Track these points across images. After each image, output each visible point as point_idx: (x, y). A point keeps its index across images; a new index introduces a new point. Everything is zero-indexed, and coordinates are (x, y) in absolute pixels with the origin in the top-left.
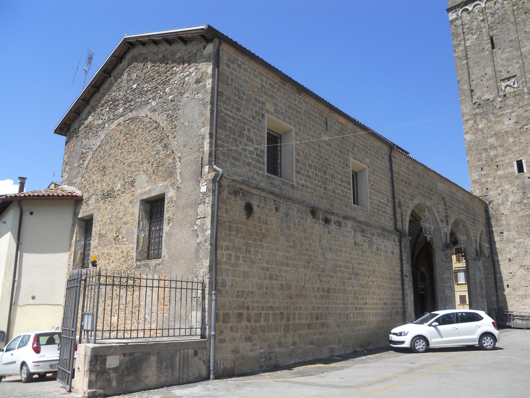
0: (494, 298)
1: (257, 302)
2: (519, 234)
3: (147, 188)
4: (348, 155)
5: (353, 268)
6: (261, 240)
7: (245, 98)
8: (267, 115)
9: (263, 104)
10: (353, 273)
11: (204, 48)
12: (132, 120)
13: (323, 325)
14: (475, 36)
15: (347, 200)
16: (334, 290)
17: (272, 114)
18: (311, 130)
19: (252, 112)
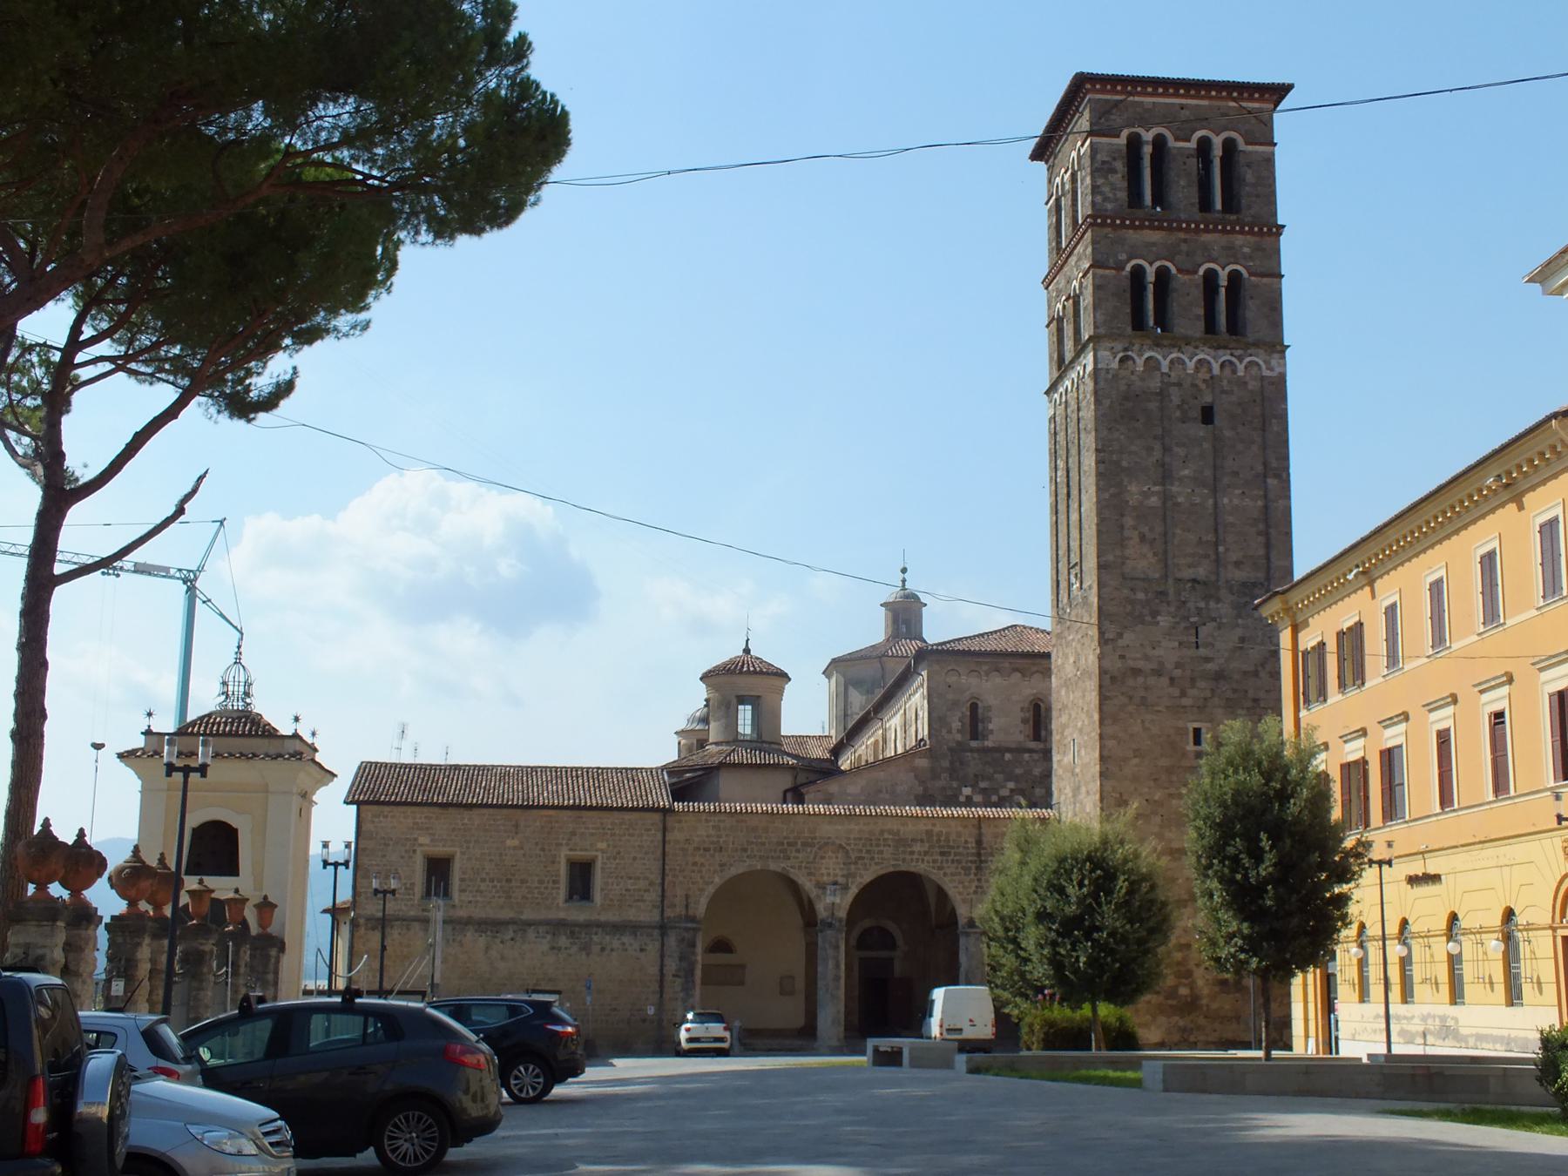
8: (419, 850)
9: (416, 839)
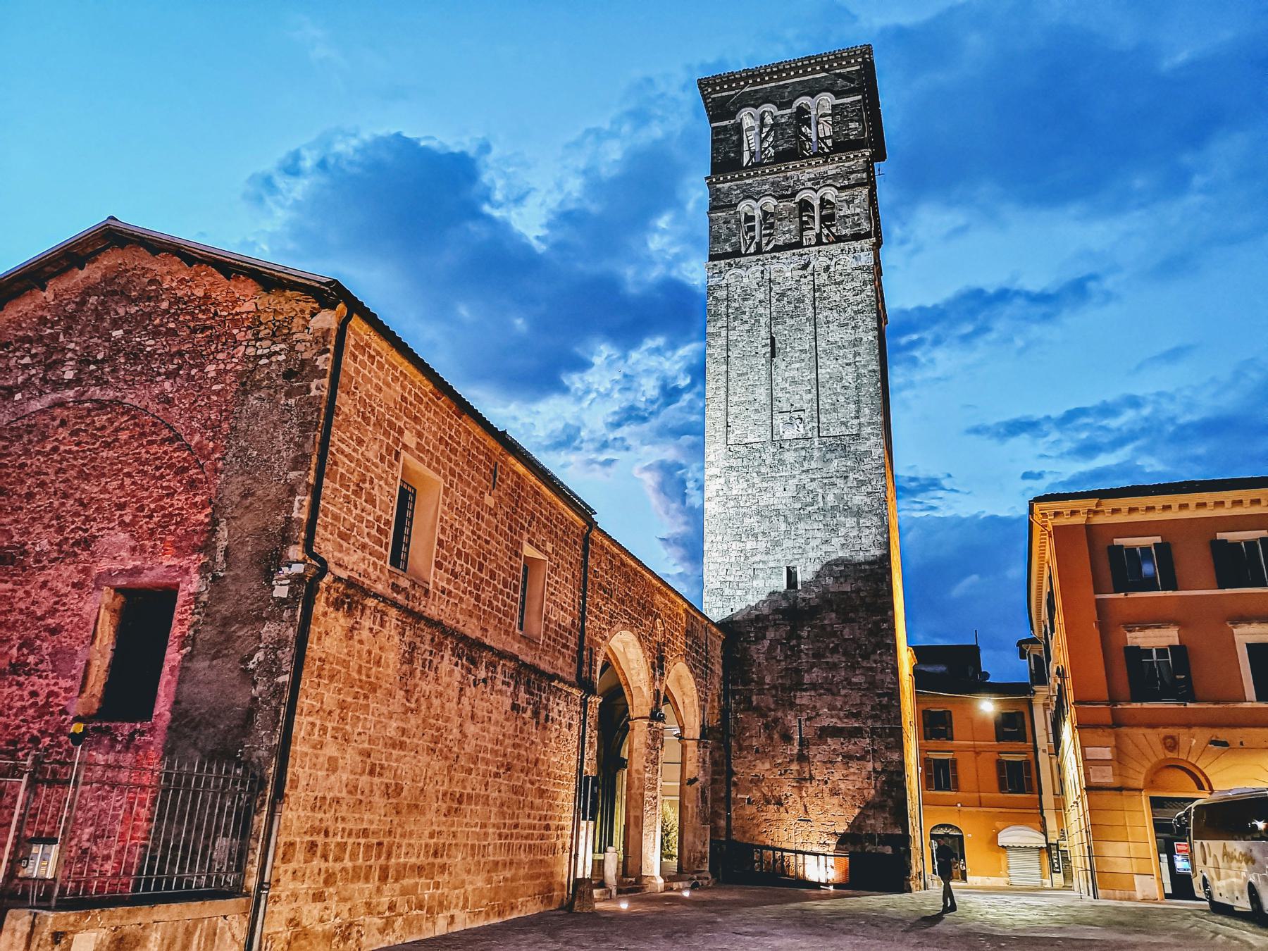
0: (723, 823)
1: (343, 819)
2: (776, 703)
3: (130, 566)
4: (521, 535)
5: (505, 755)
6: (366, 697)
7: (373, 419)
9: (401, 432)
10: (503, 765)
11: (313, 315)
12: (101, 405)
13: (443, 868)
14: (747, 327)
15: (508, 620)
16: (470, 797)
17: (412, 454)
18: (469, 484)
19: (381, 447)
